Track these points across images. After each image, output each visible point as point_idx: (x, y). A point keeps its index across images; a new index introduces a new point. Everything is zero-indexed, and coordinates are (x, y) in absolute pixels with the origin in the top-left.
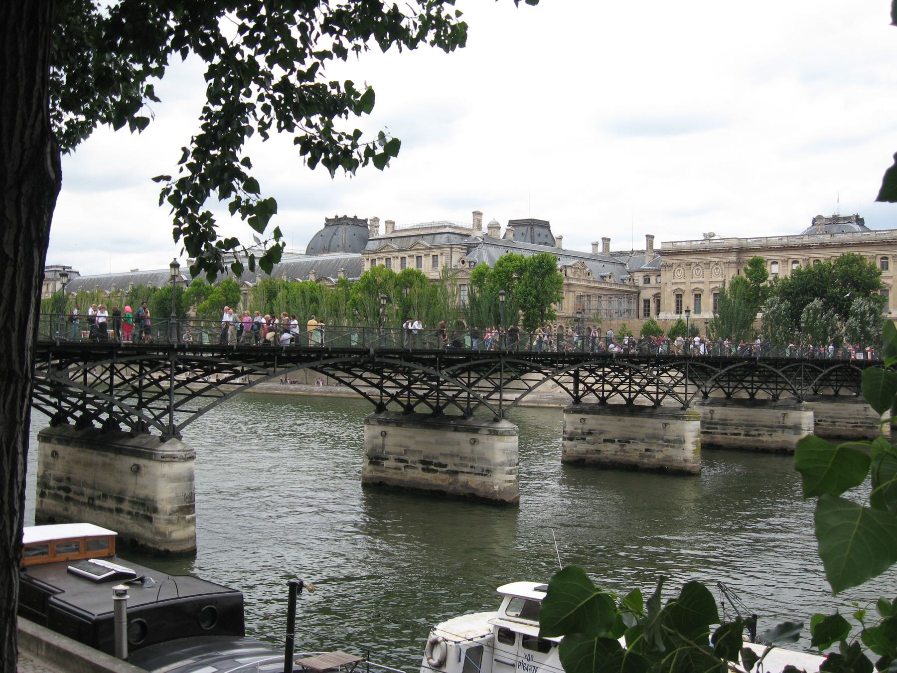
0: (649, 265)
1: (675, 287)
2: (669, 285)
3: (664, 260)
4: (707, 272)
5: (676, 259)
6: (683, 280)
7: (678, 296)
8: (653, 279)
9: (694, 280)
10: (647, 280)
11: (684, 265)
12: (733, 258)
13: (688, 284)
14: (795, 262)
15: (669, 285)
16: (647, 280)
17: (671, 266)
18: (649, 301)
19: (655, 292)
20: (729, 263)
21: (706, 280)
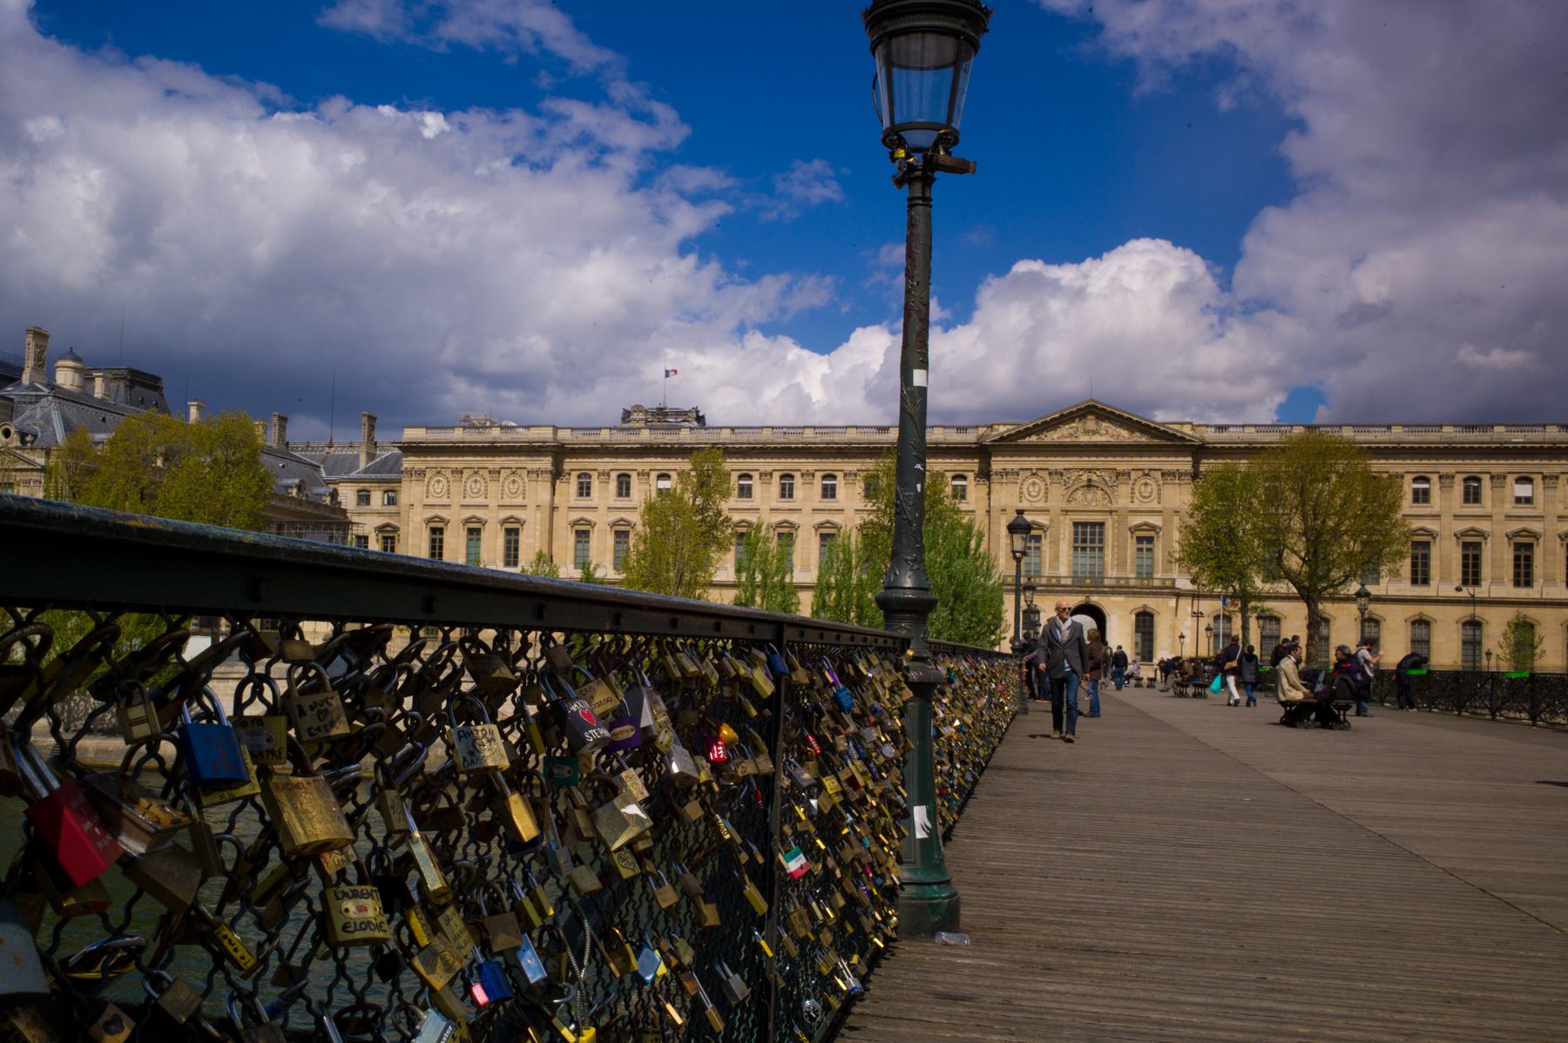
0: (366, 471)
1: (430, 513)
2: (418, 508)
3: (410, 462)
4: (493, 487)
5: (432, 461)
6: (445, 501)
7: (434, 531)
8: (377, 498)
9: (468, 501)
10: (364, 498)
11: (448, 473)
12: (546, 463)
13: (456, 508)
14: (664, 476)
15: (418, 508)
16: (364, 498)
17: (422, 473)
18: (366, 538)
19: (380, 521)
20: (538, 472)
21: (493, 502)
